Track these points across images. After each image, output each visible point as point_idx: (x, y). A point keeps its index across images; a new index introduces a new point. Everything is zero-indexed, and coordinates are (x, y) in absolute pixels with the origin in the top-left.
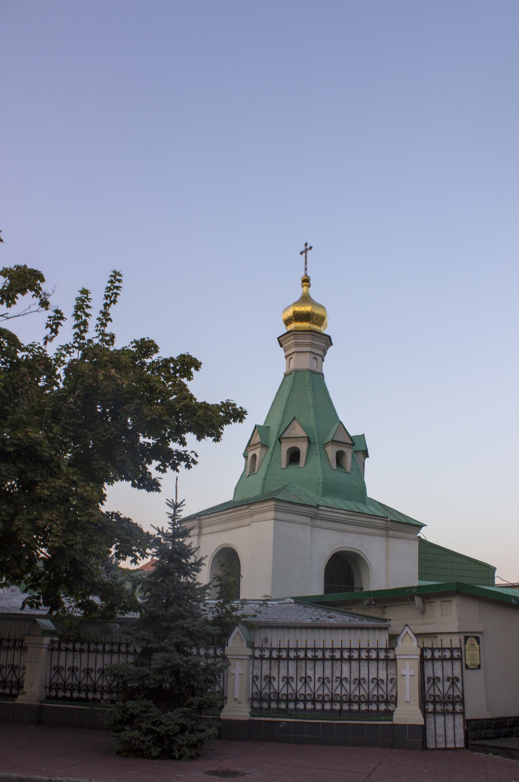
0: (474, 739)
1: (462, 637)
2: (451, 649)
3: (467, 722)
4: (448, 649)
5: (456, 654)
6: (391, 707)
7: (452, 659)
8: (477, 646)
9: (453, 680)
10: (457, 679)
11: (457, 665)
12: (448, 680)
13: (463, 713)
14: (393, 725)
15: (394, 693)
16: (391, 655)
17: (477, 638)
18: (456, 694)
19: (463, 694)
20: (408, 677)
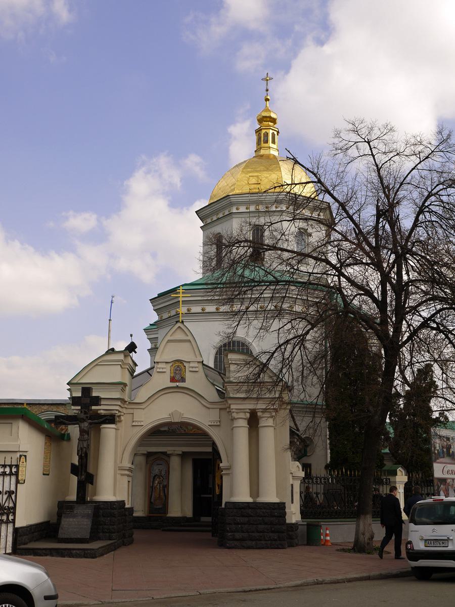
0: (19, 545)
1: (18, 455)
2: (11, 466)
3: (16, 531)
4: (9, 465)
5: (14, 470)
7: (11, 474)
8: (25, 463)
9: (10, 493)
10: (13, 492)
11: (13, 478)
12: (6, 493)
13: (14, 521)
17: (25, 456)
18: (10, 506)
19: (15, 504)
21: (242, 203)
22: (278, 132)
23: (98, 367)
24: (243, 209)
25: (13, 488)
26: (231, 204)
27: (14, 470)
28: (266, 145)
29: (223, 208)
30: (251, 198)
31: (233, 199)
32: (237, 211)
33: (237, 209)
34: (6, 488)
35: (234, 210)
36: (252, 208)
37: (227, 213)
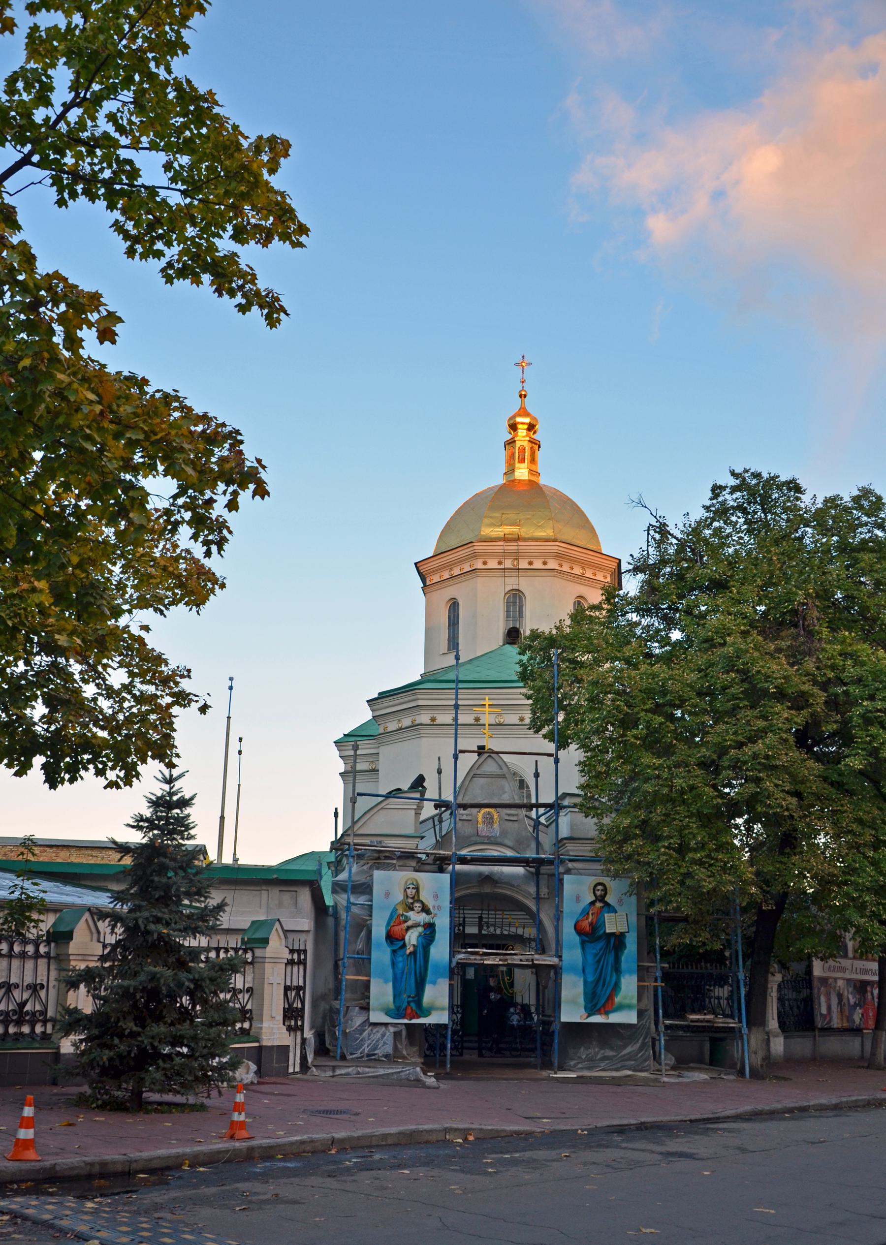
5: (302, 957)
6: (246, 1025)
14: (260, 1048)
15: (249, 1007)
16: (249, 956)
20: (275, 985)
21: (492, 555)
22: (539, 447)
23: (385, 811)
24: (493, 564)
25: (301, 984)
26: (475, 556)
27: (302, 957)
28: (522, 465)
29: (461, 561)
30: (506, 548)
31: (479, 547)
32: (484, 567)
33: (485, 563)
34: (295, 984)
35: (479, 565)
36: (508, 564)
37: (467, 568)
